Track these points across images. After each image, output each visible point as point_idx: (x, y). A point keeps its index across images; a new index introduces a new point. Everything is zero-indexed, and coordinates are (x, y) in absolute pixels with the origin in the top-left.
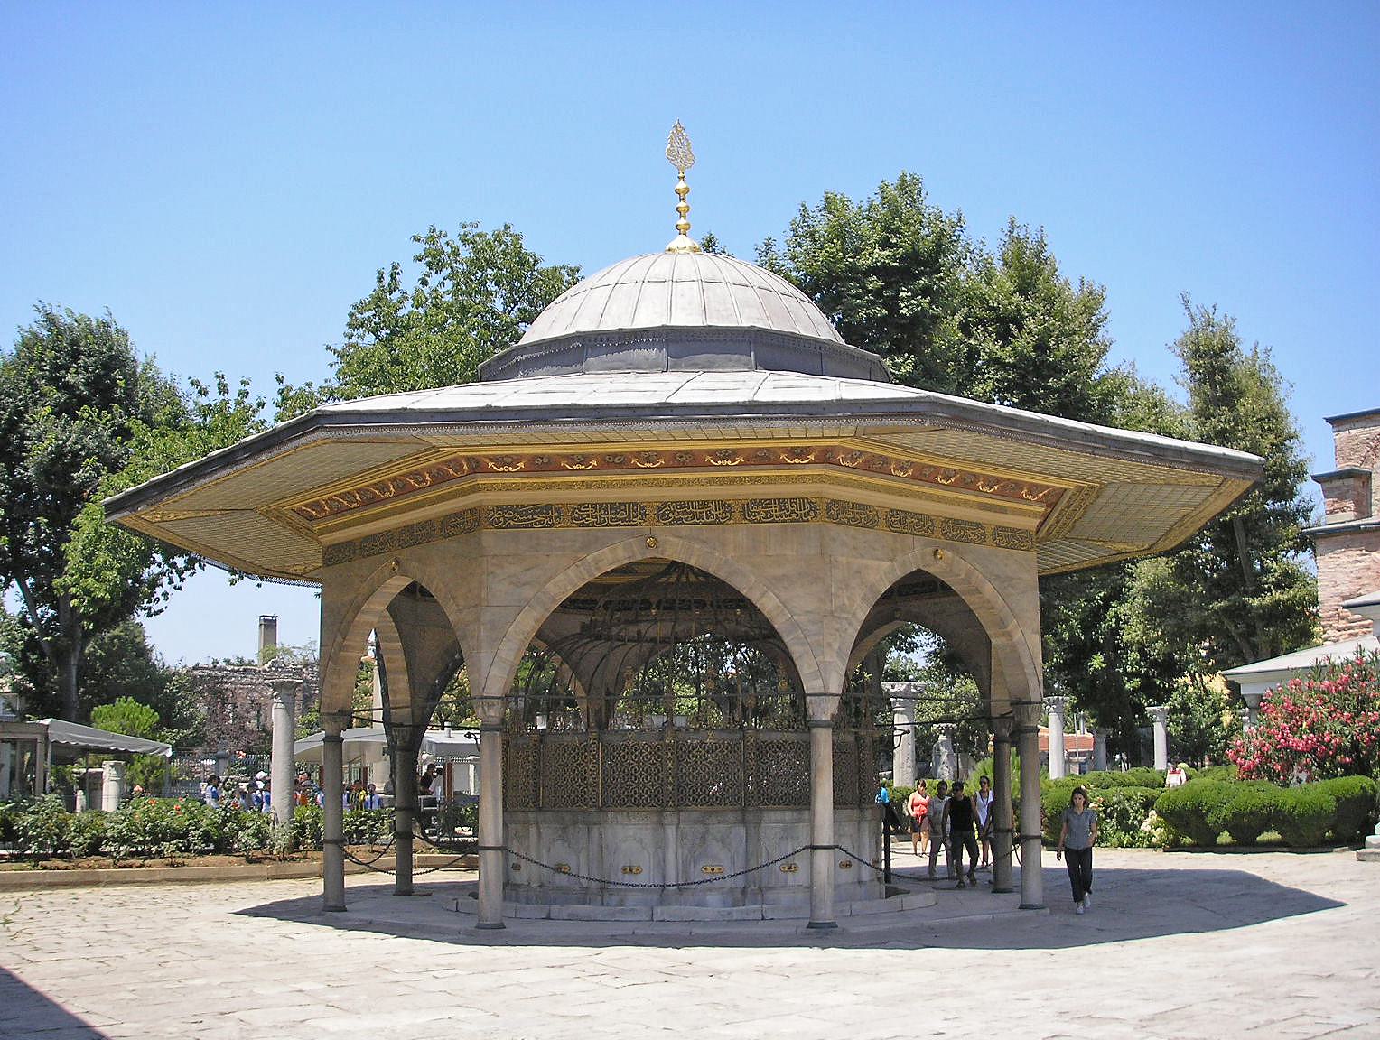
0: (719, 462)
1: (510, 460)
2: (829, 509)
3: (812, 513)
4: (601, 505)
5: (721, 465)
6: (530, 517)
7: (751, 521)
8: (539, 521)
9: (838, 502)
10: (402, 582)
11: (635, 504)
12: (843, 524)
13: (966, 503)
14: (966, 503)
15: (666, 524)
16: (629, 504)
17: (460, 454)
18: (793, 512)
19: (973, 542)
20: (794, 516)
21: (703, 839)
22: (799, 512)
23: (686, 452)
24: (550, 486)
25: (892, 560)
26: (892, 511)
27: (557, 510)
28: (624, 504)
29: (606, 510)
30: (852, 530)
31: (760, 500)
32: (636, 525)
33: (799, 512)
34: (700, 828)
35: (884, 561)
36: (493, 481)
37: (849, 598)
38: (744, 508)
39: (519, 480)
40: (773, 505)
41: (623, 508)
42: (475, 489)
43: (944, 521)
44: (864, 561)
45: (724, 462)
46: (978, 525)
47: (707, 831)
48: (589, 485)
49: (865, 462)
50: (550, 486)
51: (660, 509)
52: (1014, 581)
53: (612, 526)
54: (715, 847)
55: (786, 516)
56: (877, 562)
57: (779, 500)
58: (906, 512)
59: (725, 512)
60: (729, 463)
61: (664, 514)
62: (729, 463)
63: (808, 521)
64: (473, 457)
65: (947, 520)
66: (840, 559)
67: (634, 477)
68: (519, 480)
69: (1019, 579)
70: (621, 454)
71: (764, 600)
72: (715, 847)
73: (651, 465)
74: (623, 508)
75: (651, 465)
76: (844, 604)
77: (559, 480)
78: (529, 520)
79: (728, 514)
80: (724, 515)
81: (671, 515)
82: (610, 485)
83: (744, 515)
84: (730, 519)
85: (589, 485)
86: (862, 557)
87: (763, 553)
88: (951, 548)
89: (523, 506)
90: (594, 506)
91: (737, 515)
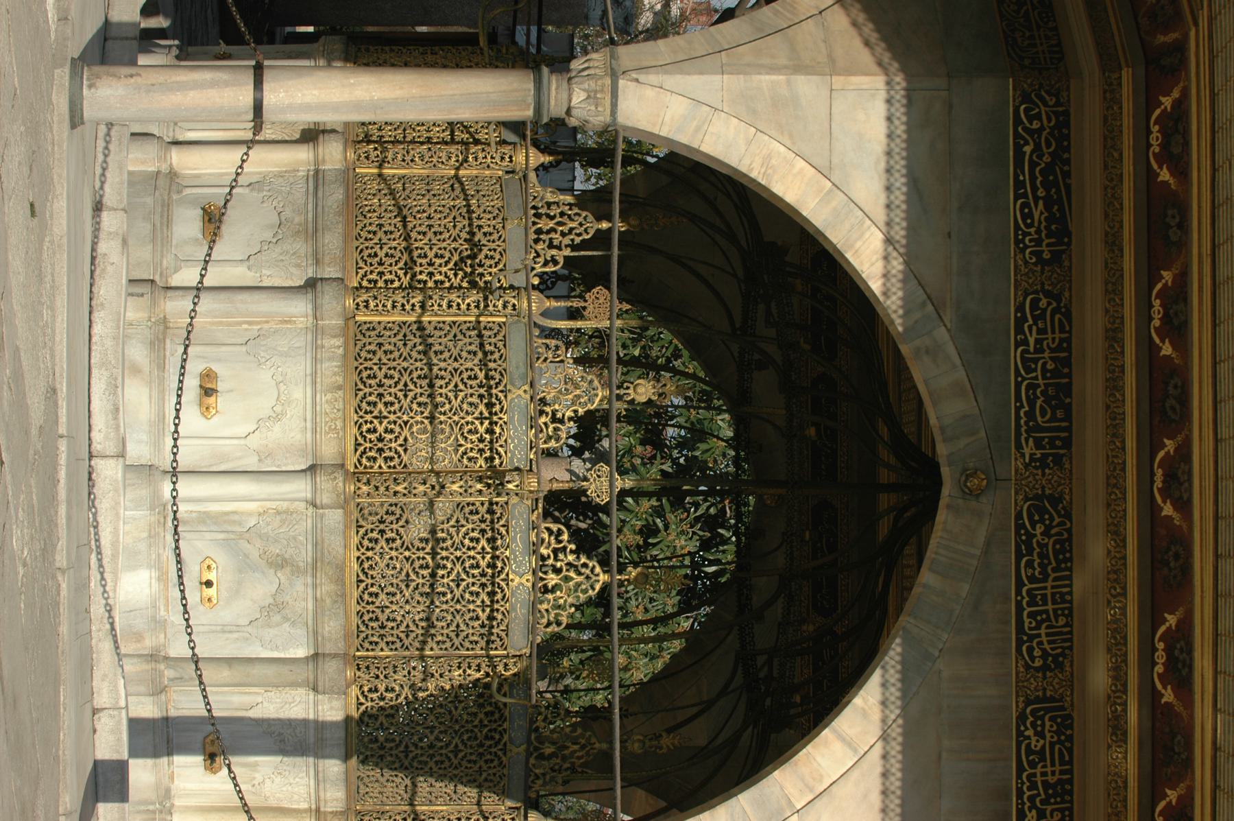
0: (1161, 646)
1: (1176, 150)
4: (1067, 362)
5: (1154, 650)
6: (1041, 193)
7: (1022, 718)
8: (1031, 215)
11: (1067, 443)
15: (1019, 516)
16: (1068, 429)
17: (1192, 33)
21: (280, 563)
23: (1186, 570)
24: (1113, 243)
27: (1056, 257)
28: (1068, 417)
29: (1056, 373)
31: (1070, 738)
32: (1019, 447)
34: (305, 555)
36: (1127, 106)
38: (1052, 699)
39: (1128, 167)
40: (1057, 768)
41: (1059, 414)
42: (1109, 63)
45: (1160, 657)
47: (297, 571)
48: (1113, 335)
50: (1113, 243)
51: (1055, 500)
53: (1018, 385)
54: (261, 588)
55: (1031, 799)
57: (1070, 782)
59: (1045, 654)
60: (1159, 669)
61: (1042, 511)
62: (1159, 669)
64: (1184, 62)
67: (1131, 444)
68: (1128, 167)
70: (1186, 416)
71: (838, 747)
72: (261, 588)
73: (1158, 483)
74: (1059, 414)
75: (1158, 483)
77: (1128, 263)
78: (1034, 189)
79: (1038, 663)
80: (1037, 653)
81: (1039, 529)
82: (1114, 385)
83: (1038, 700)
84: (1027, 667)
85: (1113, 335)
89: (1066, 175)
90: (1065, 345)
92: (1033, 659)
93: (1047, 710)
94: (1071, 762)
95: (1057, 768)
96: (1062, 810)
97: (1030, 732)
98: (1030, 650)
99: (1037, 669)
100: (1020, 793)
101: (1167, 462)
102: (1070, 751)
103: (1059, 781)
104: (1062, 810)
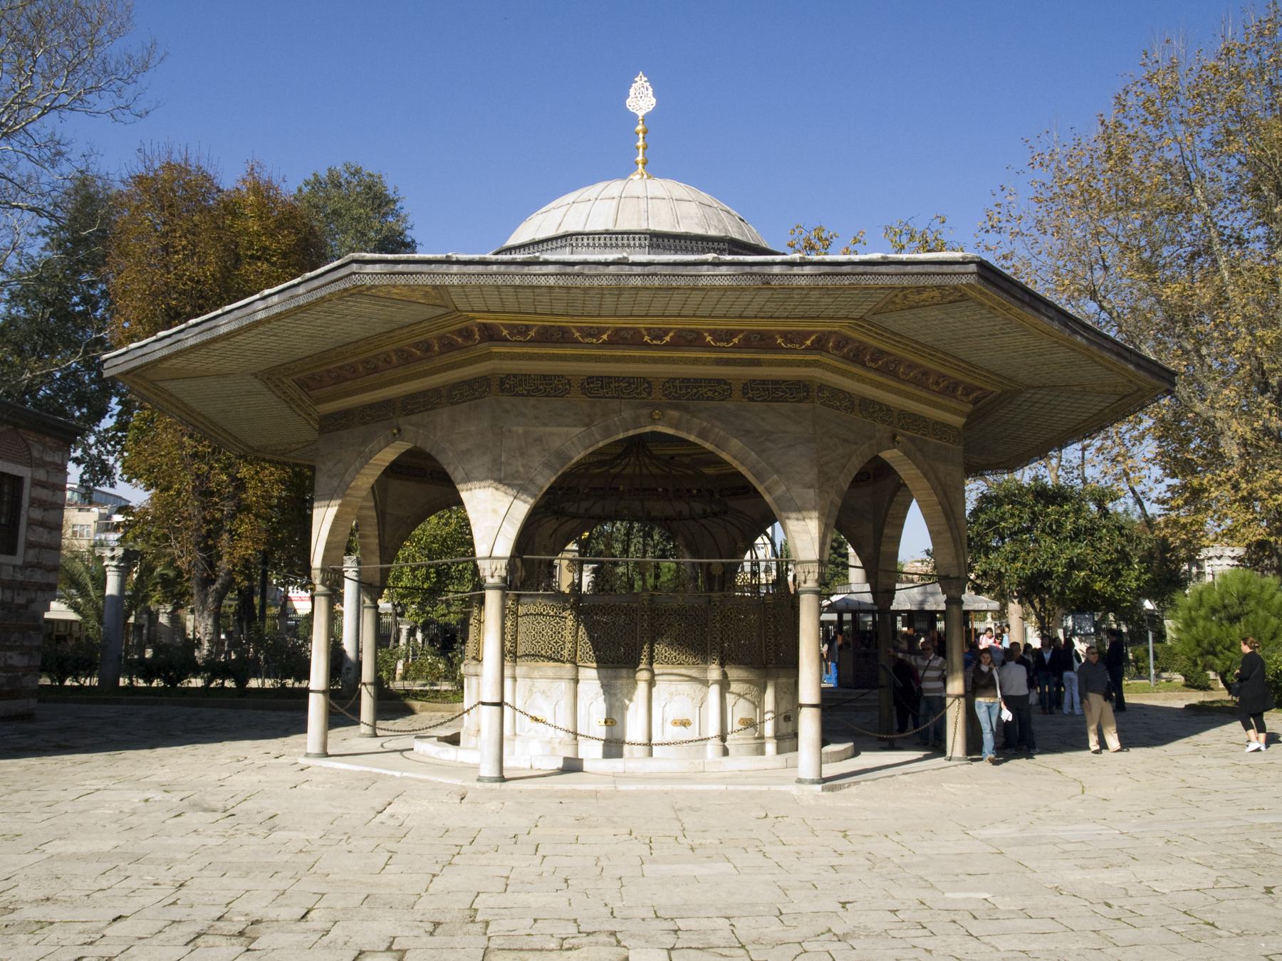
2: (502, 383)
9: (515, 376)
10: (388, 455)
12: (523, 395)
13: (695, 361)
14: (695, 361)
19: (713, 399)
25: (588, 425)
26: (591, 377)
30: (532, 401)
35: (575, 426)
37: (523, 466)
44: (548, 429)
46: (719, 381)
49: (538, 333)
56: (566, 429)
58: (609, 377)
65: (672, 380)
76: (517, 471)
86: (545, 425)
88: (676, 407)
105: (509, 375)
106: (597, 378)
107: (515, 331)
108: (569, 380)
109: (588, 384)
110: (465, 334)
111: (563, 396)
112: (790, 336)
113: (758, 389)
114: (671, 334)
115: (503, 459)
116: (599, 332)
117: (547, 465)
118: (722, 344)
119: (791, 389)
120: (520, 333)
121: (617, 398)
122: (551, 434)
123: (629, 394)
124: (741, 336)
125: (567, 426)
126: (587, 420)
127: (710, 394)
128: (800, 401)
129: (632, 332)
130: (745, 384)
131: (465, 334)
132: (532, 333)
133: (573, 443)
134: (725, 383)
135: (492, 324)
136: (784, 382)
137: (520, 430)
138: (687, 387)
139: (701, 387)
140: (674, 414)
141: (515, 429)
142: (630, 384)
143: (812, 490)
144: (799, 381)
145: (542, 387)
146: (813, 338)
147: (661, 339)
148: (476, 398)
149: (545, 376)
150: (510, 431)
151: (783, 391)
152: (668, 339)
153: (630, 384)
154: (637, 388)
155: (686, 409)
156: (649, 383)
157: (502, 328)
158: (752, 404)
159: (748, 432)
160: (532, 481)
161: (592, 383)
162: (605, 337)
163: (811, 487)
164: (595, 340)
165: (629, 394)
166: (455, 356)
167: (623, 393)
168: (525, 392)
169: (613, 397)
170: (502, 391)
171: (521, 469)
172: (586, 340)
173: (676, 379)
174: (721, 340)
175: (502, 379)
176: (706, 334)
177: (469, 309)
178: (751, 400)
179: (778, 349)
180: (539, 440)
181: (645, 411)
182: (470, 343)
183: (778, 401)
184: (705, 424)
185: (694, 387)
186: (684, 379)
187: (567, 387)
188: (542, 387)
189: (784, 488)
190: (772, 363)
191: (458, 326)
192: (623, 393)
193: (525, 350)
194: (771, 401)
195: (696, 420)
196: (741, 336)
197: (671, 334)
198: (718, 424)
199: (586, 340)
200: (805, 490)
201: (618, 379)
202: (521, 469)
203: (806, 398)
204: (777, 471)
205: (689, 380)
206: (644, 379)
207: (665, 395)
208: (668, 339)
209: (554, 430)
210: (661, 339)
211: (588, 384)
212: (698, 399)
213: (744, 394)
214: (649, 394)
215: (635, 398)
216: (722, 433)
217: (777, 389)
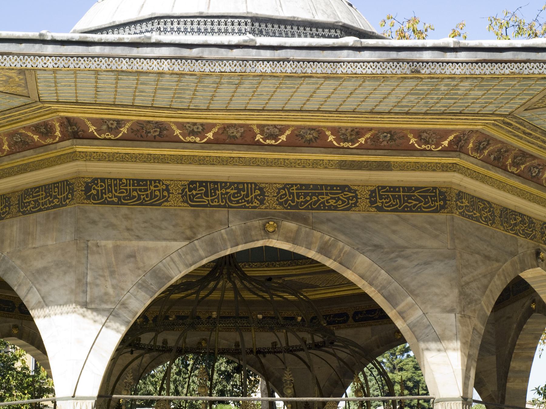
2: (88, 188)
3: (70, 196)
7: (24, 213)
9: (103, 180)
12: (113, 203)
13: (315, 164)
14: (315, 164)
18: (55, 197)
19: (336, 208)
20: (56, 201)
22: (60, 197)
25: (189, 239)
26: (192, 182)
30: (124, 210)
31: (31, 189)
33: (60, 197)
35: (175, 240)
37: (114, 287)
38: (19, 200)
43: (283, 188)
44: (142, 243)
46: (343, 188)
49: (131, 130)
52: (408, 252)
56: (164, 243)
58: (216, 183)
59: (5, 207)
63: (66, 205)
65: (287, 186)
66: (103, 243)
69: (419, 247)
71: (29, 296)
76: (106, 294)
83: (19, 207)
84: (9, 214)
86: (139, 238)
87: (30, 246)
88: (294, 218)
91: (14, 210)
92: (6, 211)
93: (22, 202)
94: (39, 187)
95: (41, 193)
96: (54, 187)
97: (29, 208)
98: (4, 213)
99: (9, 209)
100: (48, 209)
101: (338, 140)
102: (35, 188)
103: (45, 192)
104: (54, 187)
105: (96, 179)
106: (201, 183)
107: (104, 127)
108: (167, 186)
109: (190, 190)
110: (43, 130)
111: (160, 205)
112: (424, 135)
113: (388, 197)
114: (288, 132)
115: (89, 279)
116: (203, 129)
117: (142, 286)
118: (346, 145)
119: (425, 197)
120: (110, 129)
121: (224, 206)
122: (146, 249)
123: (238, 202)
124: (368, 135)
125: (165, 239)
126: (188, 233)
127: (332, 202)
128: (436, 211)
129: (242, 130)
130: (373, 192)
131: (43, 130)
132: (124, 130)
133: (172, 260)
134: (350, 190)
135: (78, 118)
136: (417, 188)
137: (110, 244)
138: (306, 195)
139: (322, 194)
140: (292, 226)
141: (103, 243)
142: (239, 191)
143: (453, 315)
144: (435, 188)
145: (135, 194)
146: (451, 138)
147: (276, 138)
148: (55, 207)
149: (139, 181)
150: (98, 246)
151: (417, 200)
152: (283, 138)
153: (239, 191)
154: (247, 196)
155: (304, 220)
156: (261, 189)
157: (89, 123)
158: (381, 214)
159: (377, 247)
160: (124, 305)
161: (195, 189)
162: (210, 135)
163: (452, 311)
164: (198, 139)
165: (238, 202)
166: (30, 157)
167: (231, 201)
168: (114, 199)
169: (219, 206)
170: (88, 198)
171: (111, 291)
172: (188, 139)
173: (292, 185)
174: (345, 140)
175: (87, 183)
176: (328, 133)
177: (54, 99)
178: (380, 209)
179: (410, 150)
180: (132, 256)
181: (257, 223)
182: (49, 141)
183: (411, 211)
184: (327, 237)
185: (314, 194)
186: (301, 185)
187: (166, 193)
188: (135, 194)
189: (421, 313)
190: (403, 167)
191: (35, 121)
192: (231, 201)
193: (115, 150)
194: (403, 211)
195: (317, 234)
196: (368, 135)
197: (288, 132)
198: (342, 237)
199: (188, 139)
200: (445, 315)
201: (225, 185)
202: (111, 291)
203: (443, 207)
204: (412, 293)
205: (307, 186)
206: (256, 184)
207: (280, 204)
208: (283, 138)
209: (151, 244)
210: (276, 138)
211: (190, 190)
212: (318, 208)
213: (372, 203)
214: (262, 202)
215: (245, 207)
216: (347, 248)
217: (409, 197)
